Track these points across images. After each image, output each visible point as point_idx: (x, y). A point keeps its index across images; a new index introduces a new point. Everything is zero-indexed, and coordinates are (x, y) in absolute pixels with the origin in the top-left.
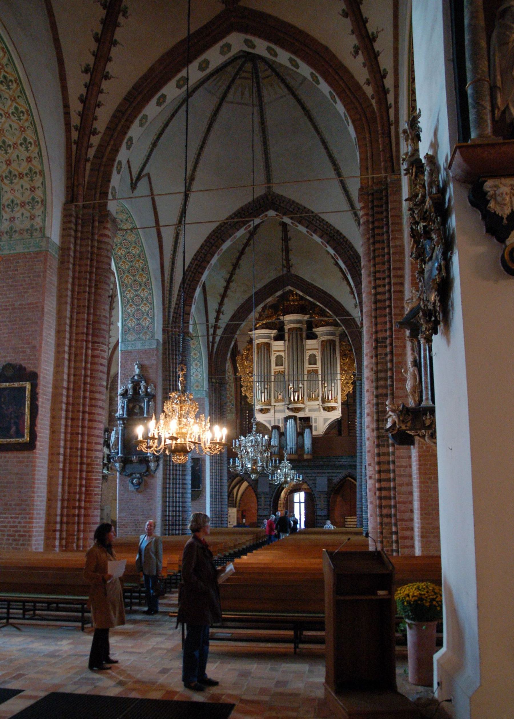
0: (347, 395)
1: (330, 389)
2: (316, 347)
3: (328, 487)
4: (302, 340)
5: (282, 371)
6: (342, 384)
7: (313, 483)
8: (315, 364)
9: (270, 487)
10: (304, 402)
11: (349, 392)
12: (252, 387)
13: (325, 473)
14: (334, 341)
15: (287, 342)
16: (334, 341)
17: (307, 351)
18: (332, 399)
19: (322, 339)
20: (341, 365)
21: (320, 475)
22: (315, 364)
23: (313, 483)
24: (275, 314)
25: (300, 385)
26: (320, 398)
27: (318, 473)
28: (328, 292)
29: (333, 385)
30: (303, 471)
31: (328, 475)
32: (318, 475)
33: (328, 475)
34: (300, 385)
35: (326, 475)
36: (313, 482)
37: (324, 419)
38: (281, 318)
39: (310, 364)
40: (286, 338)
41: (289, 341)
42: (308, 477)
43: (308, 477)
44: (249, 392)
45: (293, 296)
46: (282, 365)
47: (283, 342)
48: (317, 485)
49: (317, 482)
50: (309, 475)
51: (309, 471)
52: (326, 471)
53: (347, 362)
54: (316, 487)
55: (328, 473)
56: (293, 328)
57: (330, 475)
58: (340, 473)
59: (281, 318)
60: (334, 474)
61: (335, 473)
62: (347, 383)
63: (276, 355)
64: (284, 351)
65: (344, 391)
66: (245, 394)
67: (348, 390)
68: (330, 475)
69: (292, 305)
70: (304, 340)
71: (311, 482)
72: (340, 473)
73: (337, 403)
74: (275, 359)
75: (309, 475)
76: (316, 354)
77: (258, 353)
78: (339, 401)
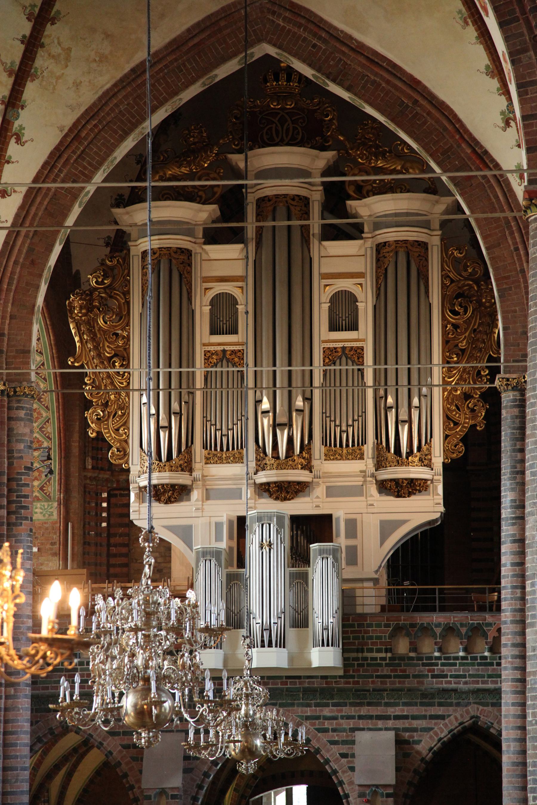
0: (464, 440)
1: (403, 416)
2: (358, 266)
3: (398, 769)
5: (233, 352)
6: (447, 400)
7: (344, 756)
8: (354, 327)
9: (186, 771)
11: (474, 426)
12: (125, 408)
13: (387, 718)
14: (424, 246)
15: (252, 247)
18: (410, 453)
20: (445, 333)
21: (370, 724)
22: (354, 327)
23: (344, 756)
25: (299, 403)
26: (369, 448)
27: (360, 717)
29: (415, 401)
30: (309, 711)
31: (400, 724)
32: (361, 724)
33: (400, 724)
34: (299, 403)
35: (390, 723)
36: (344, 749)
37: (382, 522)
39: (334, 327)
42: (326, 731)
43: (326, 731)
46: (235, 331)
47: (241, 246)
48: (358, 763)
49: (357, 749)
50: (327, 724)
51: (327, 712)
52: (391, 711)
53: (468, 322)
54: (352, 769)
55: (397, 718)
57: (405, 724)
58: (442, 717)
60: (416, 723)
61: (424, 717)
62: (467, 396)
63: (211, 294)
65: (456, 424)
67: (472, 422)
68: (405, 724)
71: (336, 750)
72: (442, 717)
73: (429, 466)
74: (207, 309)
75: (327, 724)
76: (357, 291)
78: (438, 461)
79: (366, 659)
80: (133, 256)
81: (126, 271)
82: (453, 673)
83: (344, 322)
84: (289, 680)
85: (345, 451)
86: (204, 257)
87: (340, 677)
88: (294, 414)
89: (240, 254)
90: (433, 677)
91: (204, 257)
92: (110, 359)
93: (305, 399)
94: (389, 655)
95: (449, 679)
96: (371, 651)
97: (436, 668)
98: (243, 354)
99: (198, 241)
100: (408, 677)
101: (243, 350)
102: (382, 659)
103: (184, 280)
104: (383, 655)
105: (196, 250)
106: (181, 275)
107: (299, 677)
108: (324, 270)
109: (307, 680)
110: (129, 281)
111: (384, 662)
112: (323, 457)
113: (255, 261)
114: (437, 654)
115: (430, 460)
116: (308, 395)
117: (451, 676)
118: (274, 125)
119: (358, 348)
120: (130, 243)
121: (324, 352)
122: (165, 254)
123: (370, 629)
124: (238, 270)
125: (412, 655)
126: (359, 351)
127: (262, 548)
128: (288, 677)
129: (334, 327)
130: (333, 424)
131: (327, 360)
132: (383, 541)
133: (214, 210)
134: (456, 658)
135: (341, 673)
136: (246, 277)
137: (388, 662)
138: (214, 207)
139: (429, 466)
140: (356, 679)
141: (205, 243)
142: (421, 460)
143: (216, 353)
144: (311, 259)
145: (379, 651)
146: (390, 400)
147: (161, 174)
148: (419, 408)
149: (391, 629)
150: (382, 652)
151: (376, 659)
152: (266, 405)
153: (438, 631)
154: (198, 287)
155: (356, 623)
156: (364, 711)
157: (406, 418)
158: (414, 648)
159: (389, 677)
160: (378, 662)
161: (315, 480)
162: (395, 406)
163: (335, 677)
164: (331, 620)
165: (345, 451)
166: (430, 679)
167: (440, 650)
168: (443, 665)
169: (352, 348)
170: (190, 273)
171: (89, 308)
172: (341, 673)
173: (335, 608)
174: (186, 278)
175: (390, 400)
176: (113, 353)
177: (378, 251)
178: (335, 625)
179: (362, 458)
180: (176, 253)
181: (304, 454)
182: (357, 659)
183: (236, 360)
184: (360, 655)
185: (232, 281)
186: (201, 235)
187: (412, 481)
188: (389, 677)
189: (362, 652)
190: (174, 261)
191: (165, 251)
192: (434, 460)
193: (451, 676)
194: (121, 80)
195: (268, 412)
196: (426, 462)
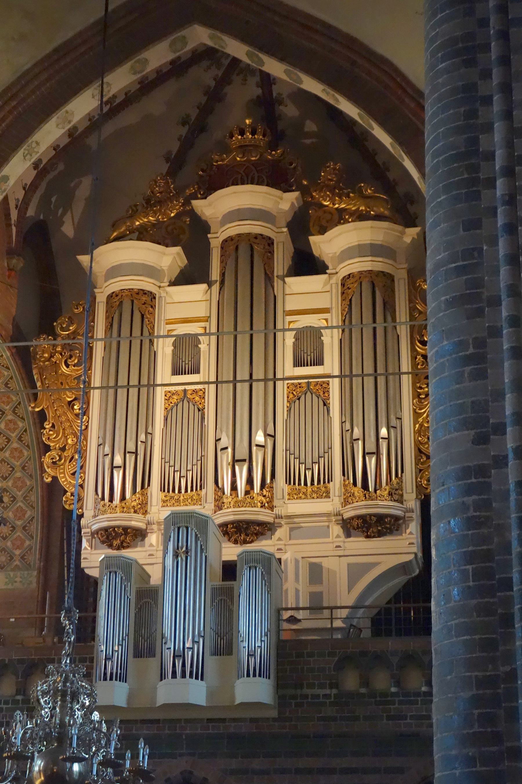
2: (323, 302)
4: (269, 279)
5: (195, 391)
8: (319, 361)
10: (271, 501)
14: (389, 278)
15: (216, 288)
16: (389, 278)
17: (289, 318)
19: (343, 273)
22: (319, 361)
24: (179, 191)
28: (344, 27)
29: (384, 432)
34: (259, 438)
38: (197, 204)
40: (215, 274)
41: (222, 283)
44: (69, 468)
45: (242, 133)
46: (196, 370)
47: (204, 286)
51: (256, 764)
56: (239, 235)
59: (197, 204)
64: (207, 319)
66: (55, 479)
69: (240, 164)
70: (277, 284)
74: (169, 350)
77: (109, 327)
79: (306, 697)
80: (98, 303)
81: (91, 318)
82: (414, 713)
83: (309, 358)
84: (210, 725)
85: (309, 490)
86: (169, 300)
87: (274, 720)
88: (254, 448)
89: (204, 295)
90: (389, 718)
91: (169, 300)
92: (70, 403)
93: (267, 435)
94: (334, 691)
95: (409, 721)
96: (311, 686)
97: (392, 707)
98: (204, 393)
99: (162, 285)
100: (357, 718)
101: (204, 389)
102: (325, 696)
103: (146, 320)
104: (328, 692)
105: (160, 293)
106: (143, 316)
107: (223, 720)
108: (288, 308)
109: (233, 724)
110: (93, 327)
111: (328, 701)
112: (287, 497)
113: (219, 301)
114: (393, 690)
115: (402, 495)
116: (270, 431)
117: (412, 717)
118: (240, 176)
119: (324, 382)
120: (96, 290)
121: (288, 387)
122: (127, 295)
123: (311, 659)
124: (201, 311)
125: (363, 690)
126: (324, 386)
127: (177, 557)
128: (209, 720)
129: (298, 363)
130: (297, 461)
131: (291, 396)
132: (351, 586)
133: (178, 254)
134: (418, 694)
135: (274, 714)
136: (210, 317)
137: (332, 700)
138: (178, 249)
139: (400, 501)
140: (293, 723)
141: (169, 286)
142: (390, 494)
143: (176, 393)
144: (275, 297)
145: (322, 686)
146: (357, 432)
147: (128, 224)
148: (388, 439)
149: (336, 659)
150: (325, 688)
151: (318, 696)
152: (226, 441)
153: (395, 660)
154: (162, 329)
155: (294, 652)
156: (304, 763)
157: (374, 450)
158: (365, 682)
159: (335, 719)
160: (321, 700)
161: (277, 521)
162: (362, 438)
163: (268, 719)
164: (258, 644)
165: (309, 490)
166: (385, 721)
167: (398, 683)
168: (401, 703)
169: (317, 383)
170: (153, 314)
171: (51, 353)
172: (274, 714)
173: (265, 629)
174: (147, 318)
175: (357, 432)
176: (74, 397)
177: (343, 285)
178: (264, 652)
179: (328, 497)
180: (138, 294)
181: (265, 492)
182: (294, 697)
183: (197, 398)
184: (299, 692)
185: (195, 322)
186: (166, 280)
187: (380, 518)
188: (335, 719)
189: (301, 687)
190: (135, 301)
191: (127, 293)
192: (405, 497)
193: (412, 717)
194: (42, 61)
195: (226, 448)
196: (396, 497)
